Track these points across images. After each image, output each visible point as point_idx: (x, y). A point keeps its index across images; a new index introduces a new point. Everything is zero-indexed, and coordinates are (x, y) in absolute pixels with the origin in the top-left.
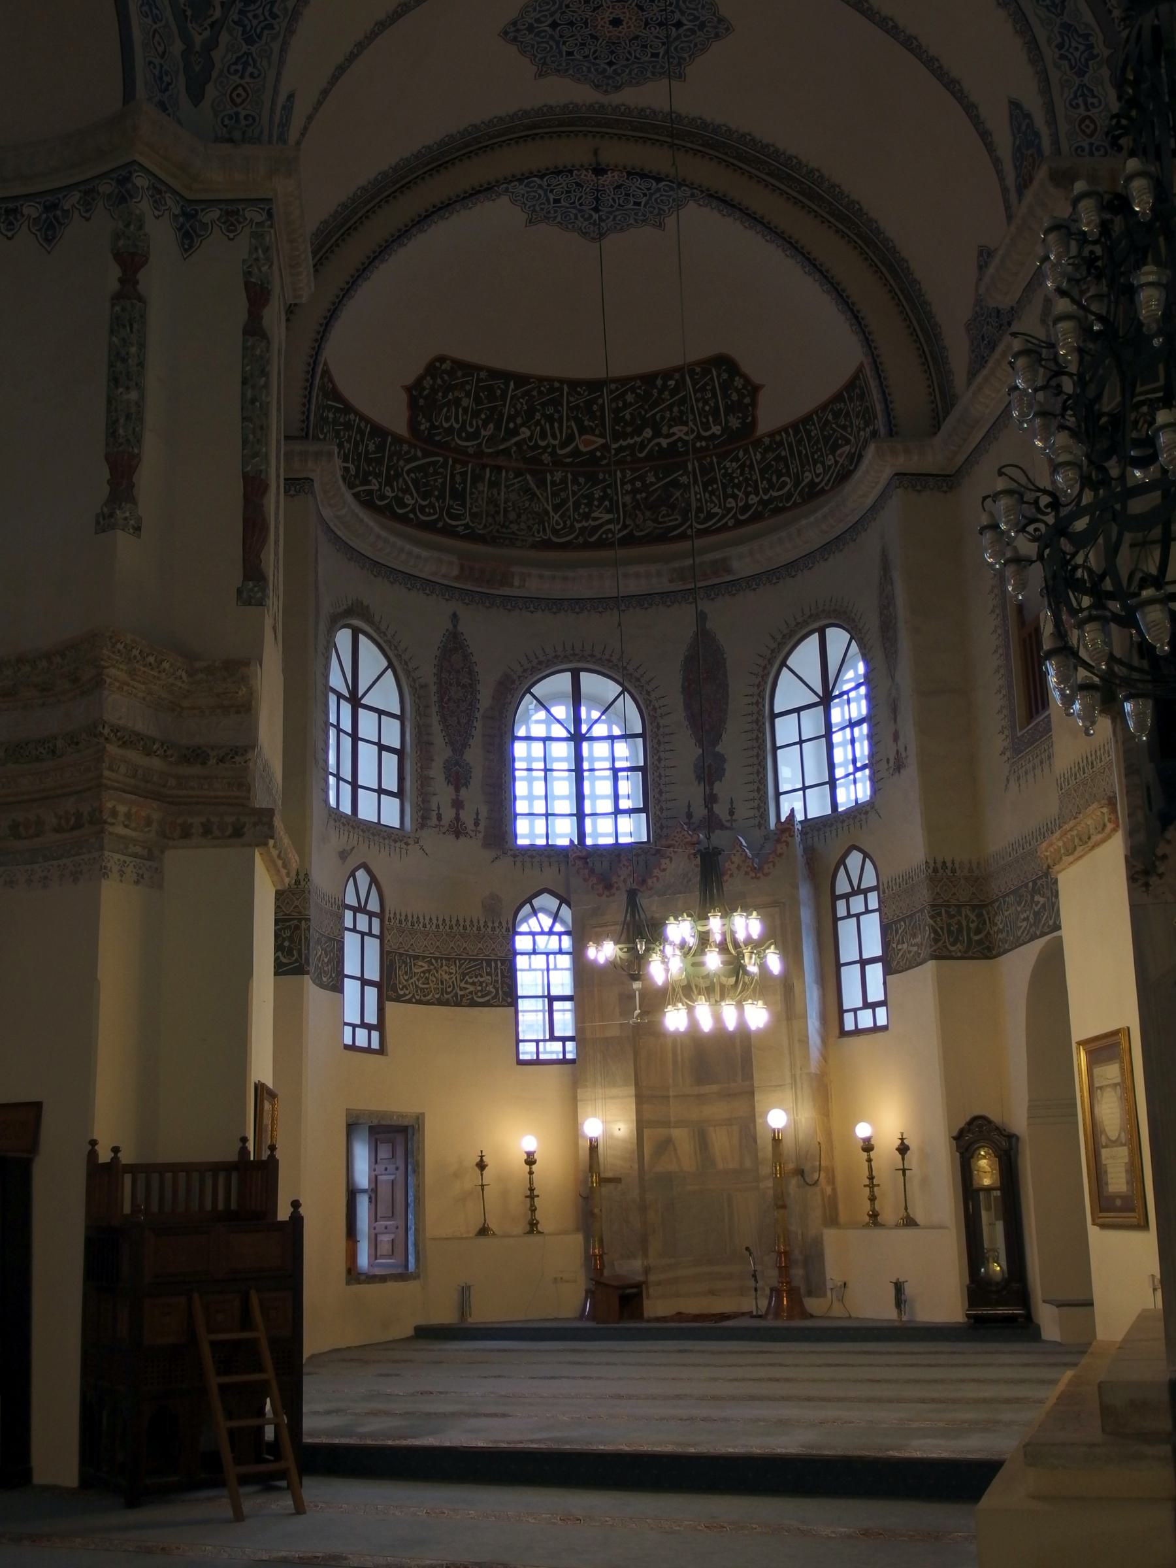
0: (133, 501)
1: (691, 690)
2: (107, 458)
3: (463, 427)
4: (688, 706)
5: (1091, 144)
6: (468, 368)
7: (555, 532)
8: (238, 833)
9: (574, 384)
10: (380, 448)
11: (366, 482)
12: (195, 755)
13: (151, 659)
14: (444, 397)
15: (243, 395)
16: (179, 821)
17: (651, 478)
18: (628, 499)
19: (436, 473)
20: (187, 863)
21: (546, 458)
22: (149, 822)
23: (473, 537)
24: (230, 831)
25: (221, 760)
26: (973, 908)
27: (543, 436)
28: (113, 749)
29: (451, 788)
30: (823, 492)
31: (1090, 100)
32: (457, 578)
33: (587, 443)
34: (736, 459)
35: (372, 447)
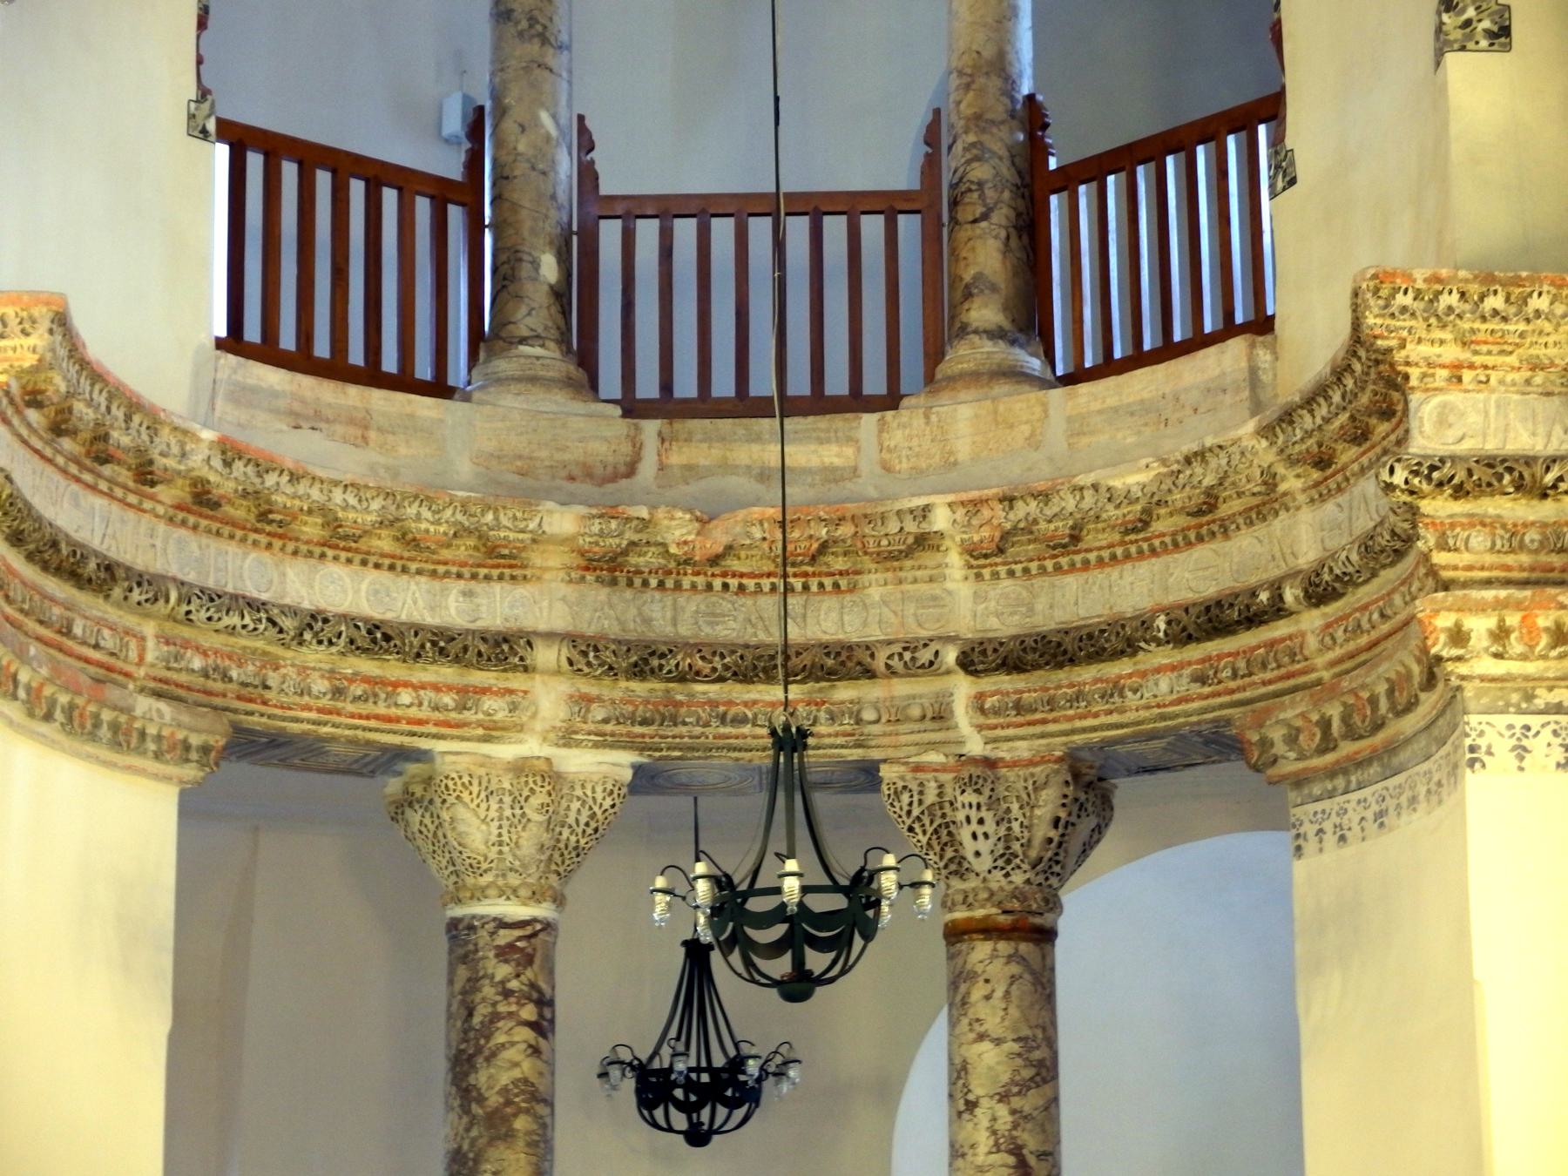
13: (1495, 302)
28: (1438, 507)
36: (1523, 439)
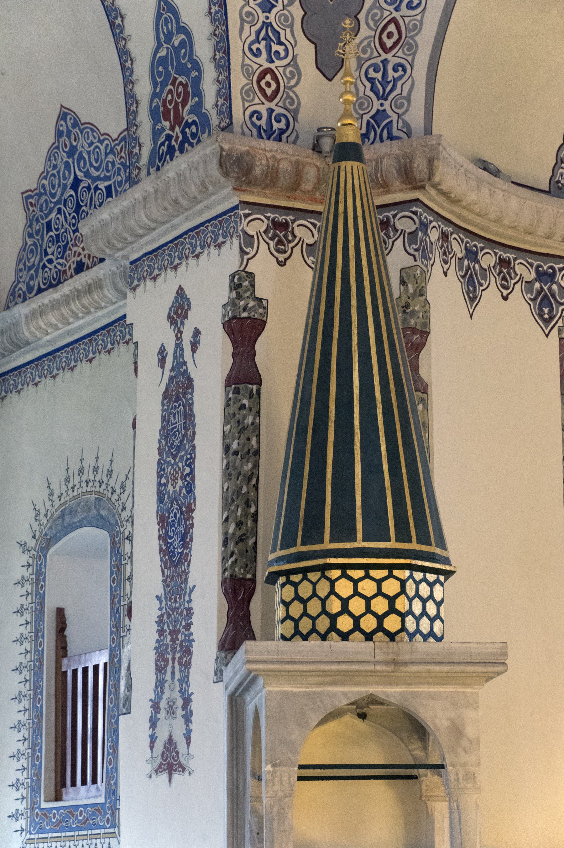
5: (270, 111)
31: (275, 47)
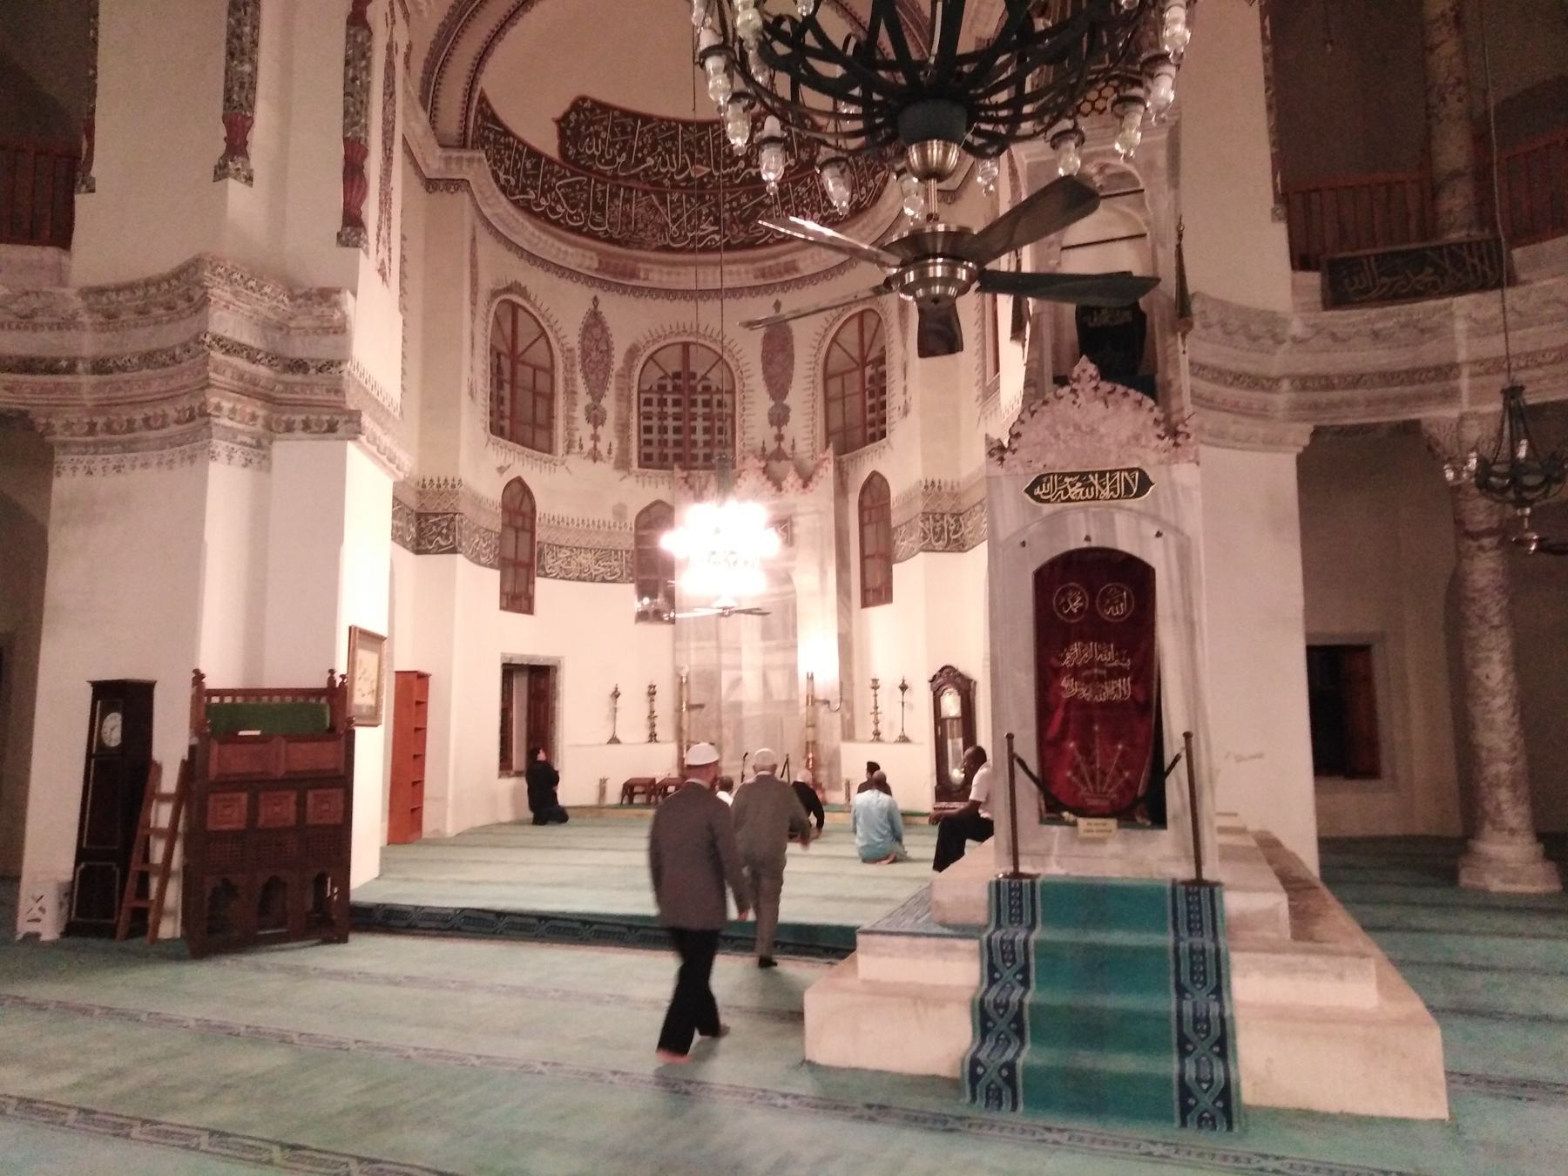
0: (246, 155)
1: (767, 361)
2: (224, 118)
3: (602, 155)
4: (765, 371)
6: (606, 108)
7: (673, 239)
8: (332, 428)
9: (686, 124)
10: (536, 166)
11: (524, 192)
12: (299, 366)
13: (252, 283)
14: (587, 128)
15: (346, 74)
16: (284, 418)
17: (744, 200)
18: (727, 215)
19: (581, 189)
20: (291, 452)
21: (666, 182)
22: (254, 417)
23: (610, 240)
24: (326, 426)
25: (320, 370)
26: (953, 515)
27: (664, 164)
28: (217, 355)
29: (590, 427)
30: (865, 208)
32: (597, 270)
33: (697, 171)
34: (805, 185)
35: (529, 165)
36: (246, 338)
